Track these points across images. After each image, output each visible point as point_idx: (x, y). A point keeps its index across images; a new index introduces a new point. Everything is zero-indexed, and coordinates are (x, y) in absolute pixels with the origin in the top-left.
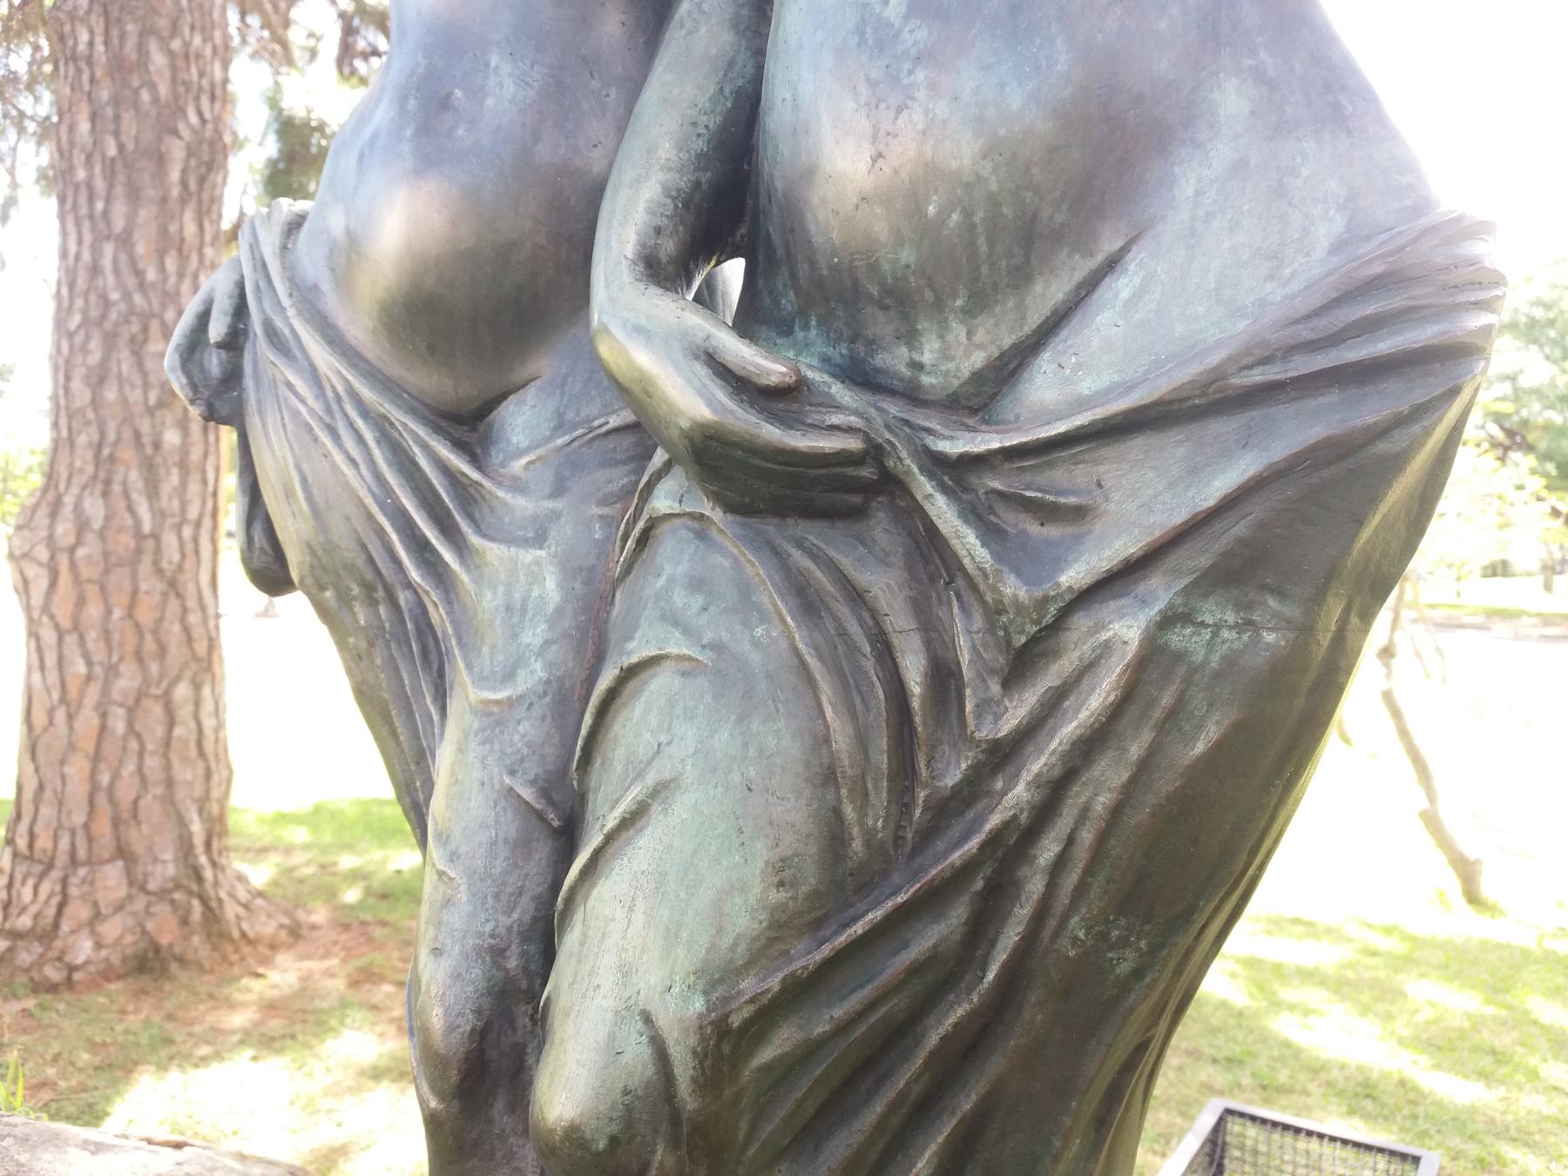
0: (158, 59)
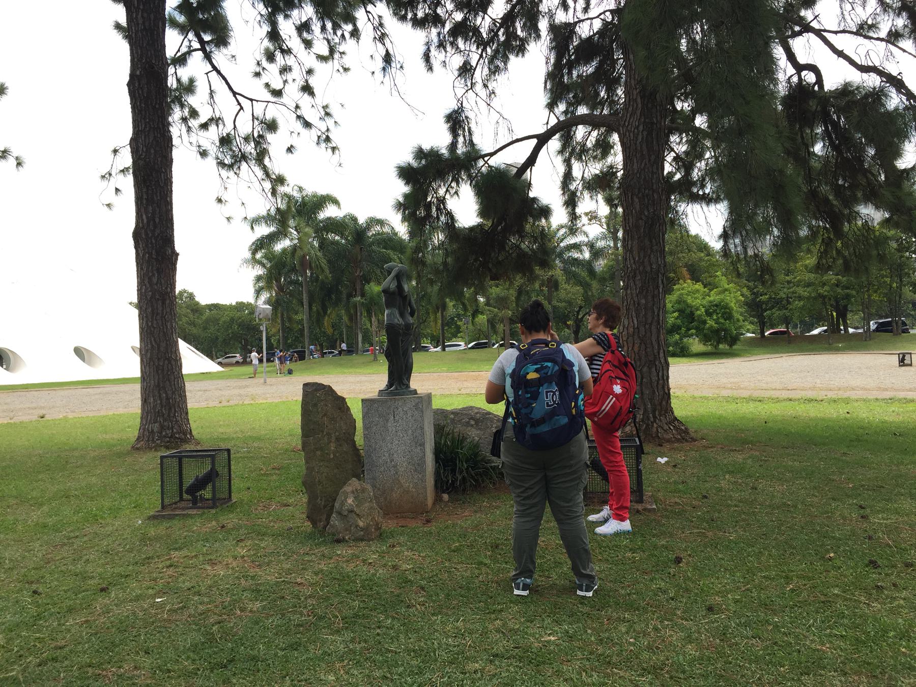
0: (636, 200)
